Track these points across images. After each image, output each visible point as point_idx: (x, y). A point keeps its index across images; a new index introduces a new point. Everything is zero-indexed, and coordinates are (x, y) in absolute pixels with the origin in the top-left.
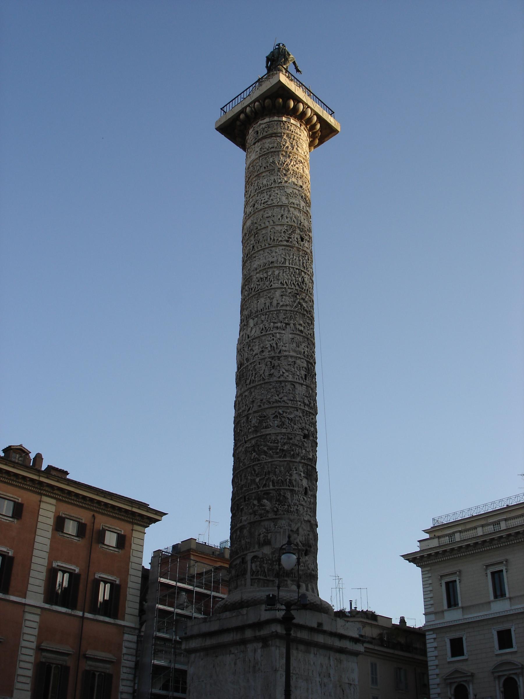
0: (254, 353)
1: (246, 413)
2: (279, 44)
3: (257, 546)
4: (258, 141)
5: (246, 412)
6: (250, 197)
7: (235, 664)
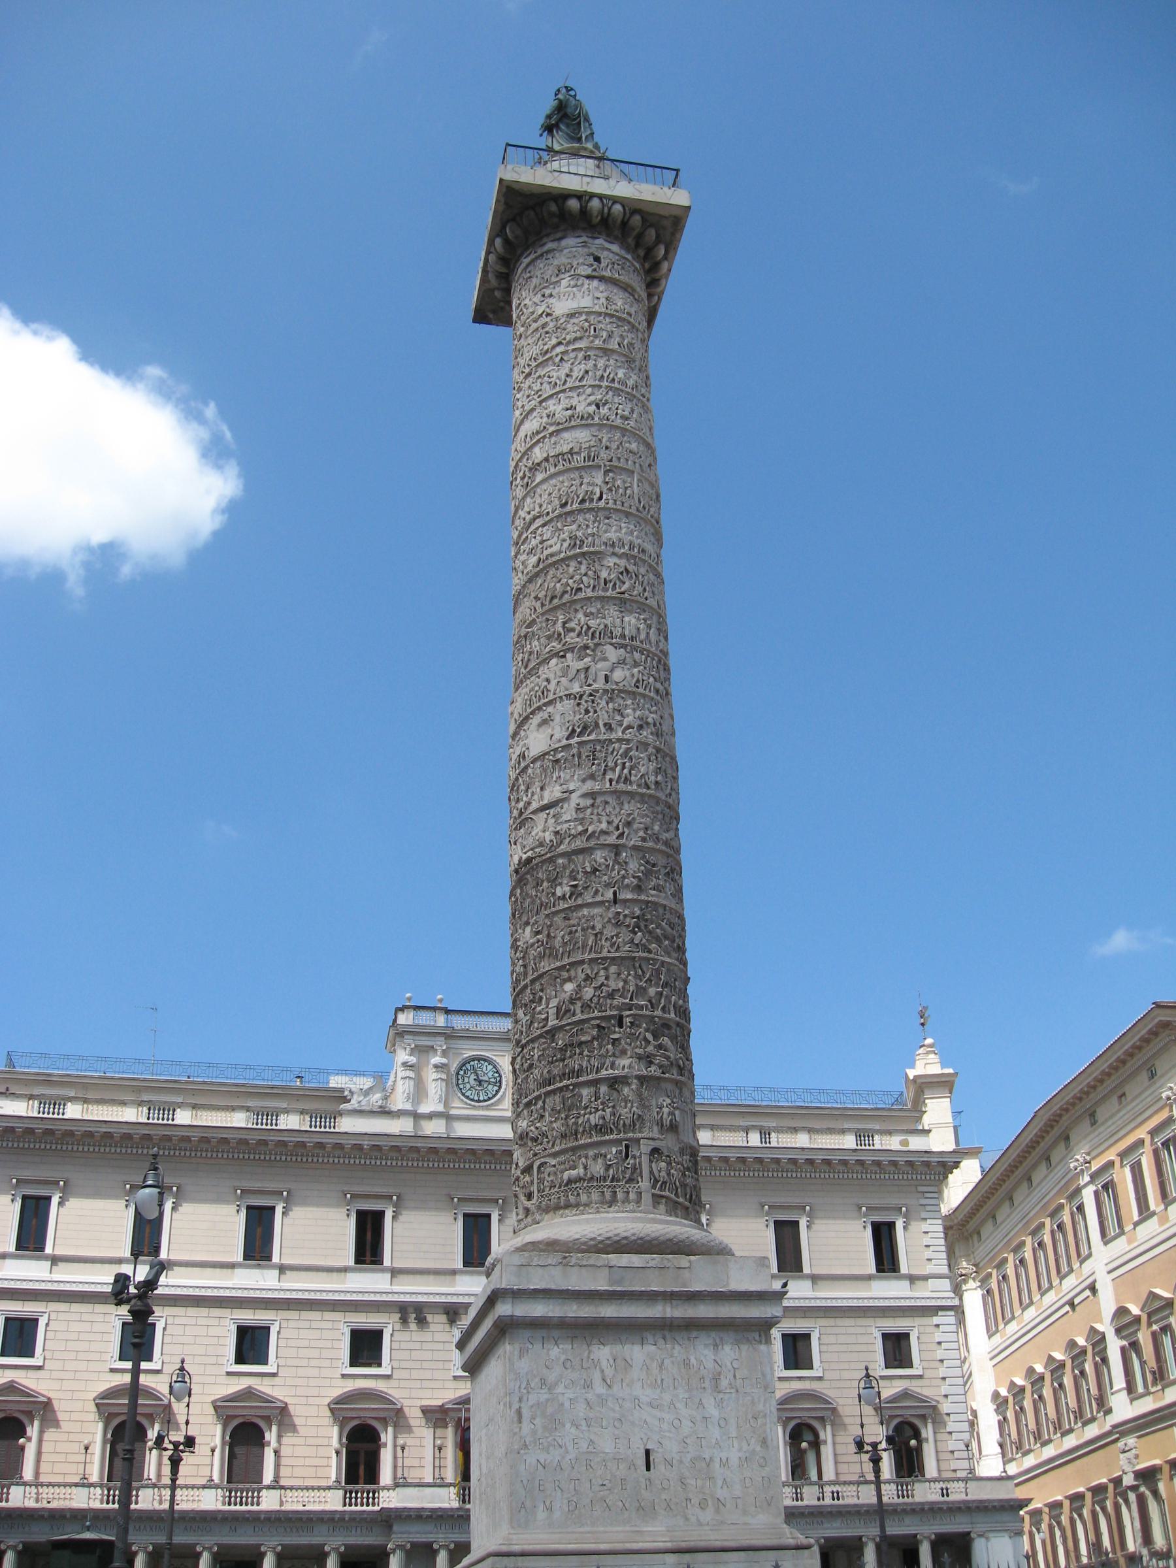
0: (625, 725)
1: (611, 839)
2: (572, 89)
3: (656, 1129)
4: (601, 279)
5: (614, 837)
6: (584, 383)
7: (661, 1366)
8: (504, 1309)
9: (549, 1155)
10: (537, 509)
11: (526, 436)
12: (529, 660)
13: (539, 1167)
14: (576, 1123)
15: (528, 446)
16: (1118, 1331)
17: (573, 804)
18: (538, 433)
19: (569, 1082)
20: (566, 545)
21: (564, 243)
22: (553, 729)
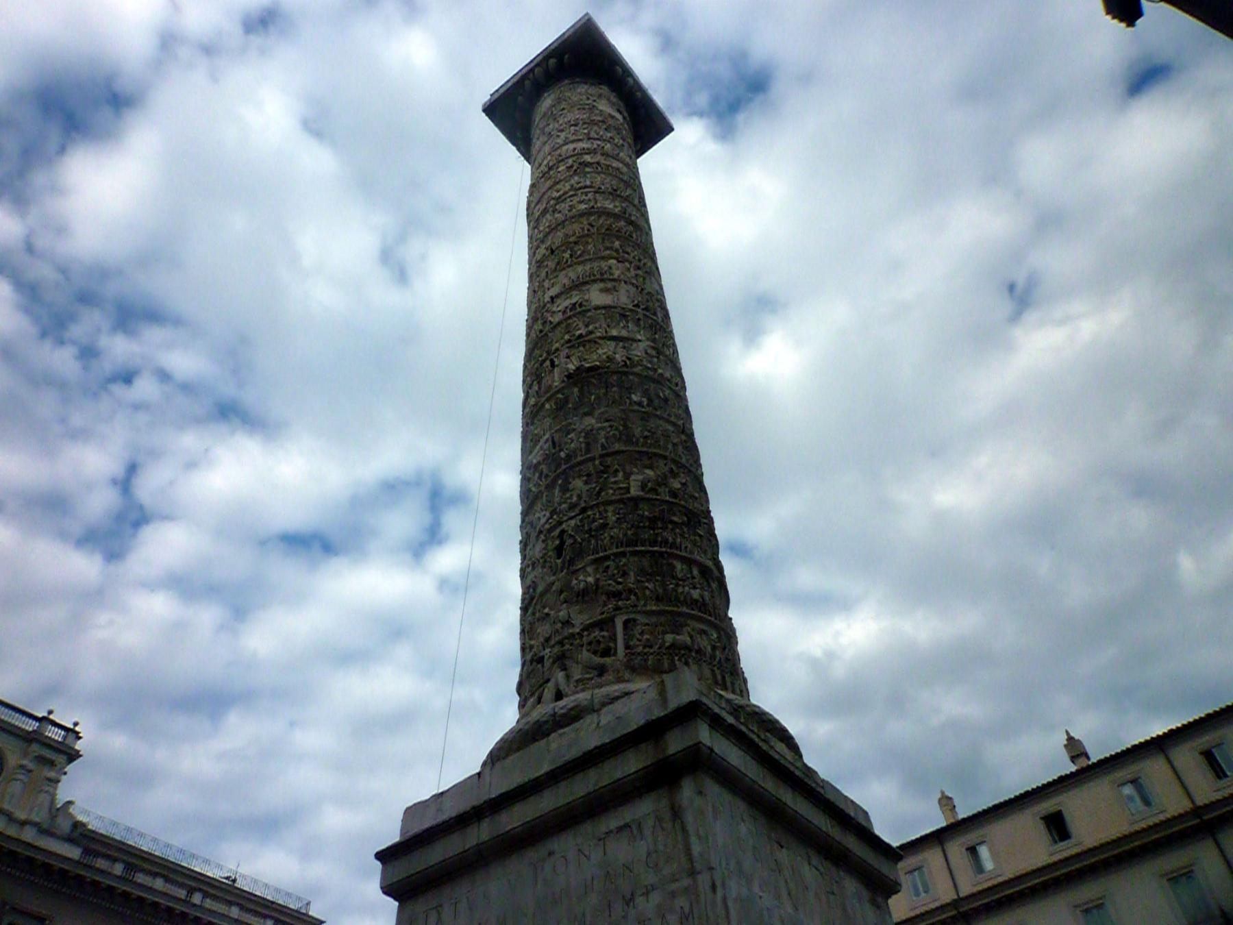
13: (626, 623)
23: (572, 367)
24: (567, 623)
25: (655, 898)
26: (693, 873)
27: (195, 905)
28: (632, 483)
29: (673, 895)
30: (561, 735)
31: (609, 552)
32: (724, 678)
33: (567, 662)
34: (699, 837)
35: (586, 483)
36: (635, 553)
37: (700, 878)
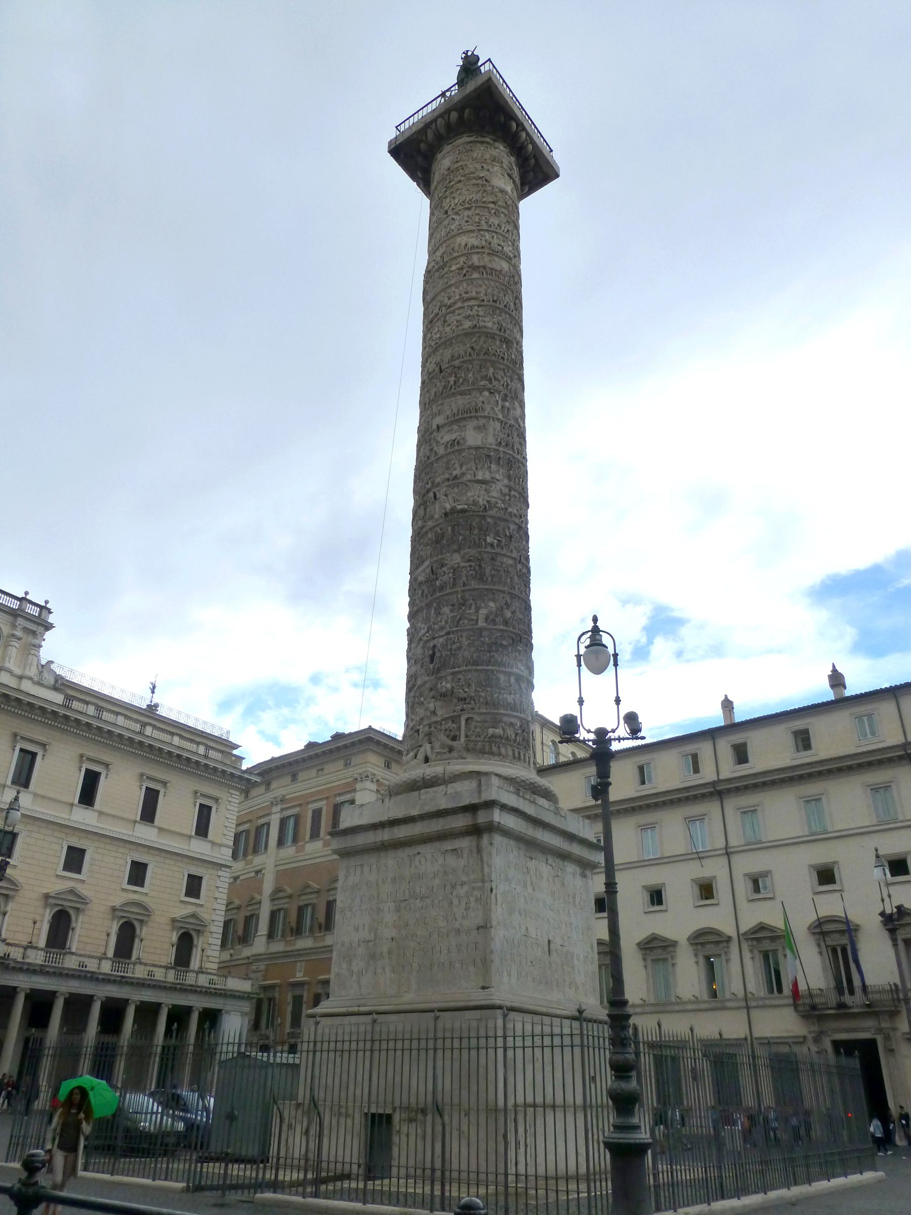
8: (498, 816)
9: (477, 713)
10: (474, 294)
11: (466, 245)
12: (462, 384)
13: (467, 720)
14: (498, 697)
15: (466, 252)
16: (273, 900)
17: (498, 488)
18: (477, 247)
19: (494, 668)
20: (496, 326)
21: (497, 144)
22: (486, 434)
23: (448, 507)
24: (434, 713)
25: (466, 888)
26: (483, 881)
27: (148, 736)
28: (480, 616)
29: (474, 888)
30: (427, 792)
31: (461, 669)
32: (519, 753)
33: (433, 739)
34: (488, 865)
35: (451, 611)
36: (477, 670)
37: (486, 884)
